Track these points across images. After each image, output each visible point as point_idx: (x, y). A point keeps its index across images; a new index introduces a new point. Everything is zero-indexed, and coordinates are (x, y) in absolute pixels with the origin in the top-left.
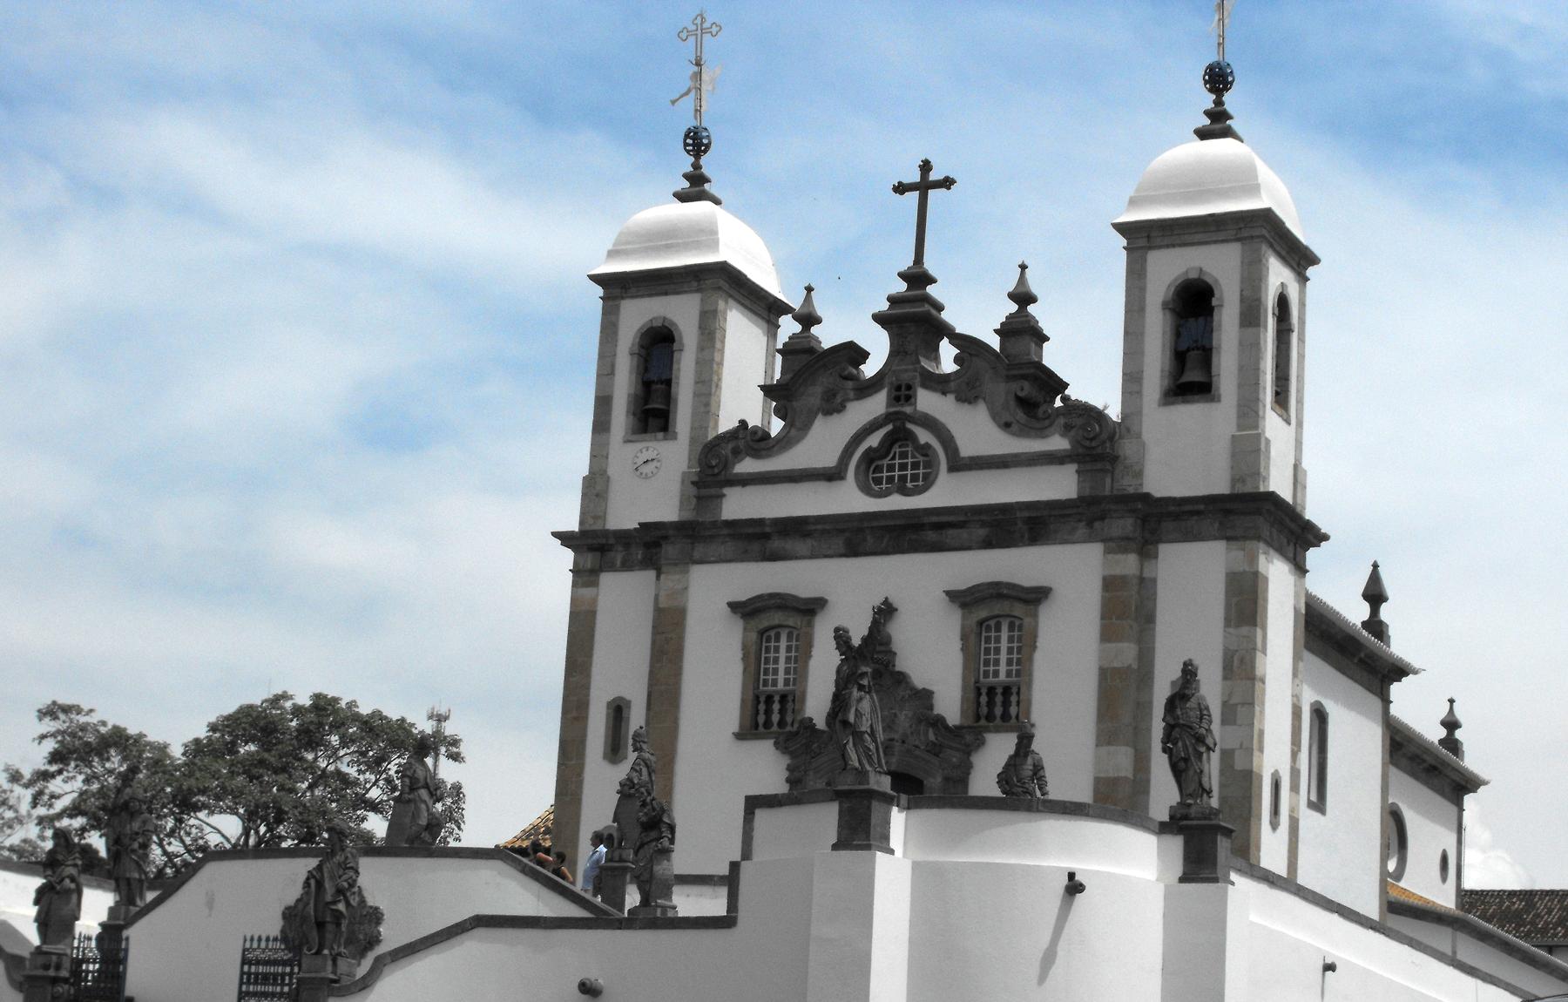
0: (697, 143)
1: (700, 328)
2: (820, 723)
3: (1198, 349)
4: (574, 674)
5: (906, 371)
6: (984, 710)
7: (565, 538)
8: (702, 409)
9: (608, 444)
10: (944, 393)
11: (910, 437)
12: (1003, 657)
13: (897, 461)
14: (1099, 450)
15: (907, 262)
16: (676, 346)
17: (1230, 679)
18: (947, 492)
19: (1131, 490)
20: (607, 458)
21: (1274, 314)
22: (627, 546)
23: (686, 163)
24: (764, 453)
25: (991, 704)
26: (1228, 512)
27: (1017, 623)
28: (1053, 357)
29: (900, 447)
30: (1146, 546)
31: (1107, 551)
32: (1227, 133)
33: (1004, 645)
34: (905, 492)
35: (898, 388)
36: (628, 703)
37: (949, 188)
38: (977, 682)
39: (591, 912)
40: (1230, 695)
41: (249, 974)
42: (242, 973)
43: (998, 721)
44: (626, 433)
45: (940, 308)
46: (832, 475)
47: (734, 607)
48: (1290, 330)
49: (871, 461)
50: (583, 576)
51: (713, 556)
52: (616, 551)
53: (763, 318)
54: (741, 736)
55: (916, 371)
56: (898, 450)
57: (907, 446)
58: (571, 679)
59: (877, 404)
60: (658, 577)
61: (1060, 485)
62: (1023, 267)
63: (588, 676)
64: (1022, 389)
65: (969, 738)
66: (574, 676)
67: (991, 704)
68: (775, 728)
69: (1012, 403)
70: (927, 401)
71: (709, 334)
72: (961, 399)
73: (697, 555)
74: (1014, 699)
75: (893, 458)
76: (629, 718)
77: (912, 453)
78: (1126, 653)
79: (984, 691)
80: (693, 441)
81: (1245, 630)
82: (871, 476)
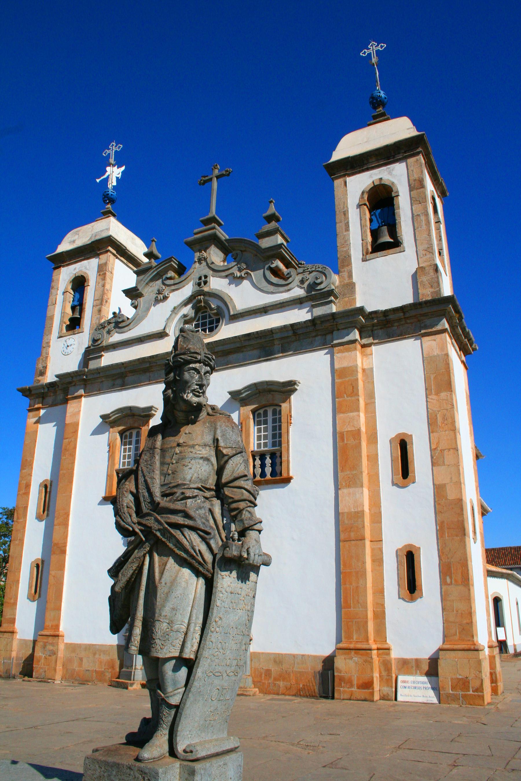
1: (98, 272)
6: (259, 471)
17: (437, 432)
21: (431, 203)
24: (126, 329)
25: (263, 466)
29: (202, 313)
35: (200, 278)
37: (228, 175)
40: (438, 443)
43: (268, 477)
52: (50, 396)
56: (201, 315)
57: (206, 312)
58: (24, 471)
63: (32, 468)
66: (25, 469)
67: (263, 466)
69: (268, 274)
71: (103, 274)
77: (209, 314)
81: (443, 395)
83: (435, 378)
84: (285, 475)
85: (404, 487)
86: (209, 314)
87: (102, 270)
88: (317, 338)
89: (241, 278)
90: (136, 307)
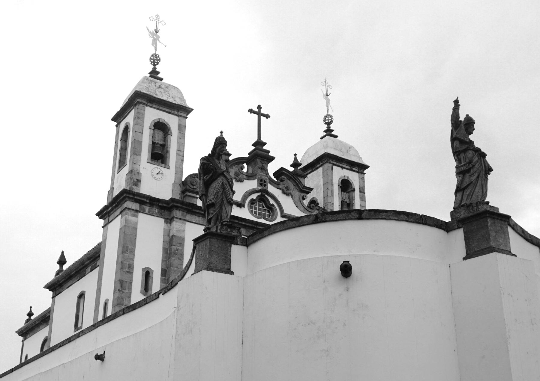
0: (155, 60)
4: (127, 252)
5: (264, 176)
8: (180, 161)
9: (140, 160)
10: (278, 188)
15: (256, 139)
16: (167, 133)
20: (140, 165)
34: (266, 219)
35: (261, 180)
37: (267, 118)
51: (194, 220)
52: (146, 206)
55: (268, 177)
57: (261, 203)
58: (126, 254)
59: (253, 184)
62: (295, 155)
63: (134, 255)
66: (128, 253)
70: (271, 188)
71: (183, 133)
72: (284, 193)
76: (153, 277)
77: (263, 205)
86: (263, 205)
89: (287, 195)
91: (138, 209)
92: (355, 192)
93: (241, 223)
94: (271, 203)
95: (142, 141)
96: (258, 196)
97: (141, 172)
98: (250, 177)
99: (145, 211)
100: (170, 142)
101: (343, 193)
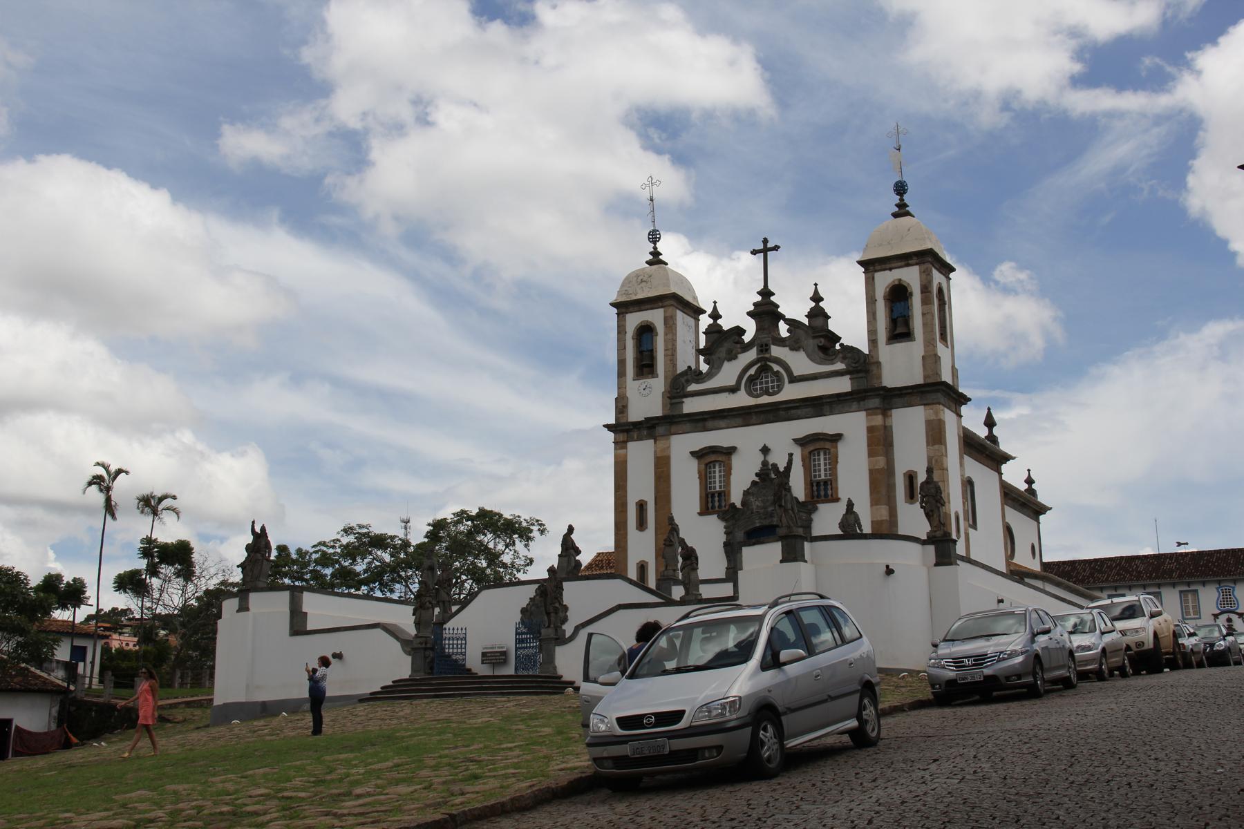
1: (665, 324)
2: (738, 505)
3: (902, 317)
5: (765, 337)
6: (816, 493)
7: (609, 427)
10: (784, 346)
11: (769, 369)
12: (822, 467)
13: (764, 380)
14: (859, 368)
15: (761, 286)
18: (790, 392)
19: (876, 386)
20: (626, 388)
22: (639, 429)
23: (650, 247)
24: (700, 381)
25: (818, 490)
26: (922, 392)
27: (827, 451)
28: (833, 326)
30: (885, 411)
31: (867, 415)
32: (908, 214)
33: (822, 462)
35: (762, 346)
36: (646, 502)
37: (777, 250)
38: (811, 480)
39: (663, 599)
41: (519, 639)
42: (516, 639)
44: (634, 376)
45: (778, 306)
46: (733, 390)
47: (692, 453)
48: (945, 304)
49: (752, 380)
50: (619, 444)
53: (692, 317)
54: (701, 514)
58: (618, 493)
59: (752, 354)
60: (655, 443)
61: (843, 385)
63: (626, 491)
64: (821, 342)
65: (810, 507)
67: (818, 490)
68: (717, 509)
69: (816, 349)
70: (776, 351)
72: (792, 349)
73: (672, 431)
74: (829, 487)
75: (762, 379)
78: (881, 462)
79: (815, 484)
80: (666, 378)
81: (936, 447)
82: (752, 388)
83: (932, 435)
84: (834, 496)
85: (912, 503)
87: (670, 323)
88: (855, 403)
90: (708, 364)
91: (625, 439)
92: (914, 298)
93: (730, 414)
94: (775, 370)
95: (625, 359)
96: (759, 367)
97: (628, 395)
98: (746, 347)
99: (634, 437)
100: (656, 345)
101: (898, 304)
